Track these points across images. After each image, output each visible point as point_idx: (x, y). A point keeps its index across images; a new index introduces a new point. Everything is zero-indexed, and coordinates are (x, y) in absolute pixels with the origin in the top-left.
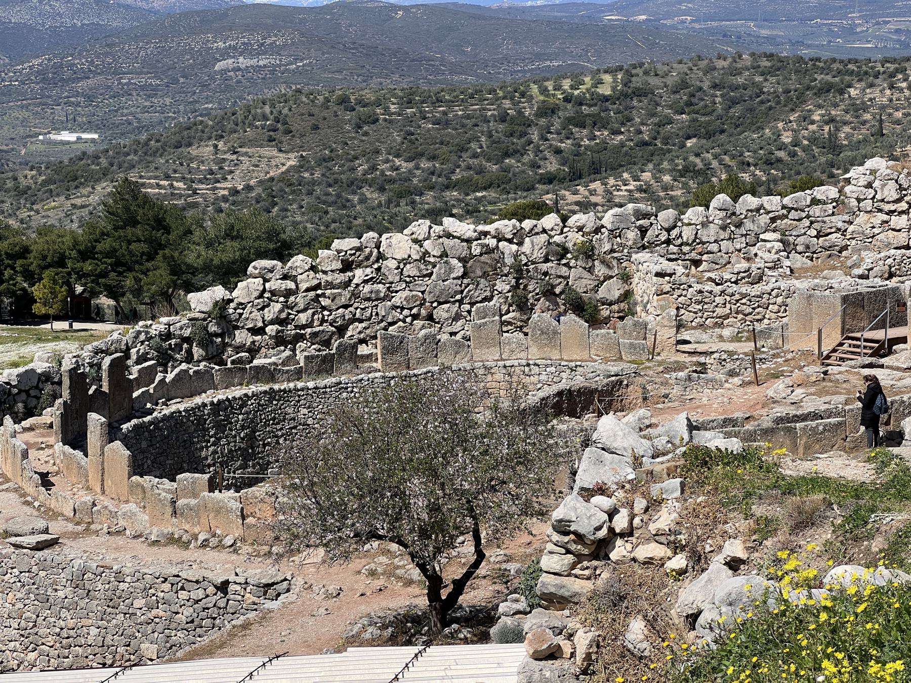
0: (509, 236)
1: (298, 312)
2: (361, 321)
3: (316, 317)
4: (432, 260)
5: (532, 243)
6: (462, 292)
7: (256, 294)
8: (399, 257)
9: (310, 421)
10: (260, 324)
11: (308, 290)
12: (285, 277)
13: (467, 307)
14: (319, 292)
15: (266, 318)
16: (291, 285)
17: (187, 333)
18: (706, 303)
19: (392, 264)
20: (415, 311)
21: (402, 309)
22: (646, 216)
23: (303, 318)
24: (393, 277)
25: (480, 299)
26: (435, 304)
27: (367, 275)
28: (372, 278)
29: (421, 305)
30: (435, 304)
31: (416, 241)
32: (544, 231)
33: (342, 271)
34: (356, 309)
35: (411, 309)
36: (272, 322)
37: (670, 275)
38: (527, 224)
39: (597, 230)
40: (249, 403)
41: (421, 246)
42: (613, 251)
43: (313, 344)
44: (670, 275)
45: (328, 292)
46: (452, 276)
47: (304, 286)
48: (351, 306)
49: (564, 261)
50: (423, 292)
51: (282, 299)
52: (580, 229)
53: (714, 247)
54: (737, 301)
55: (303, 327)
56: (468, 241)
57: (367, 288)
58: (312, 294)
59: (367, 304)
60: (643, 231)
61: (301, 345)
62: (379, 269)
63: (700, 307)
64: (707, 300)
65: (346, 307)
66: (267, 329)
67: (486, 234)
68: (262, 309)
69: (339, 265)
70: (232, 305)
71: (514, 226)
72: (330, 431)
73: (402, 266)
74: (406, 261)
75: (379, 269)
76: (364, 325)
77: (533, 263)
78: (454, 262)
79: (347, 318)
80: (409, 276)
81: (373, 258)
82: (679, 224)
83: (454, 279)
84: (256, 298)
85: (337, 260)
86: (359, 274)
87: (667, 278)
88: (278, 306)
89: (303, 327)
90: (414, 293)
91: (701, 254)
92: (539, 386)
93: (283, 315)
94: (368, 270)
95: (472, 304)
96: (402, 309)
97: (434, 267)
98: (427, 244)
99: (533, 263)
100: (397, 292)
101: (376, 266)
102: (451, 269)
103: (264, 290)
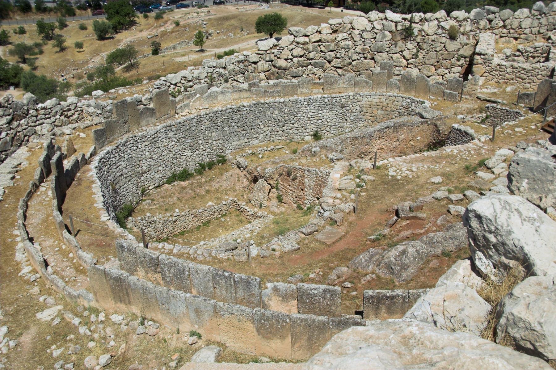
0: (417, 21)
1: (309, 52)
2: (339, 58)
3: (317, 55)
4: (376, 31)
6: (389, 47)
9: (279, 118)
10: (290, 57)
11: (315, 42)
13: (391, 55)
14: (320, 43)
15: (294, 55)
18: (501, 71)
19: (357, 32)
20: (365, 55)
21: (360, 53)
22: (494, 13)
23: (312, 55)
24: (357, 38)
25: (398, 51)
26: (376, 53)
31: (370, 21)
35: (363, 54)
36: (296, 57)
37: (484, 55)
38: (428, 15)
39: (465, 20)
40: (245, 109)
41: (372, 24)
42: (471, 31)
43: (315, 67)
44: (484, 55)
45: (324, 44)
49: (444, 35)
51: (302, 46)
52: (455, 19)
53: (528, 31)
54: (519, 72)
55: (312, 59)
56: (396, 22)
58: (317, 44)
59: (343, 50)
60: (490, 21)
61: (310, 67)
63: (497, 73)
64: (501, 70)
65: (332, 51)
66: (294, 59)
67: (405, 19)
69: (331, 31)
70: (278, 48)
71: (420, 16)
73: (361, 33)
74: (363, 31)
76: (340, 60)
77: (427, 35)
78: (387, 33)
81: (347, 29)
82: (511, 18)
84: (290, 45)
86: (340, 36)
87: (482, 56)
89: (312, 59)
91: (520, 35)
92: (401, 108)
93: (302, 53)
96: (360, 53)
97: (376, 34)
98: (375, 23)
99: (427, 35)
101: (348, 33)
102: (385, 36)
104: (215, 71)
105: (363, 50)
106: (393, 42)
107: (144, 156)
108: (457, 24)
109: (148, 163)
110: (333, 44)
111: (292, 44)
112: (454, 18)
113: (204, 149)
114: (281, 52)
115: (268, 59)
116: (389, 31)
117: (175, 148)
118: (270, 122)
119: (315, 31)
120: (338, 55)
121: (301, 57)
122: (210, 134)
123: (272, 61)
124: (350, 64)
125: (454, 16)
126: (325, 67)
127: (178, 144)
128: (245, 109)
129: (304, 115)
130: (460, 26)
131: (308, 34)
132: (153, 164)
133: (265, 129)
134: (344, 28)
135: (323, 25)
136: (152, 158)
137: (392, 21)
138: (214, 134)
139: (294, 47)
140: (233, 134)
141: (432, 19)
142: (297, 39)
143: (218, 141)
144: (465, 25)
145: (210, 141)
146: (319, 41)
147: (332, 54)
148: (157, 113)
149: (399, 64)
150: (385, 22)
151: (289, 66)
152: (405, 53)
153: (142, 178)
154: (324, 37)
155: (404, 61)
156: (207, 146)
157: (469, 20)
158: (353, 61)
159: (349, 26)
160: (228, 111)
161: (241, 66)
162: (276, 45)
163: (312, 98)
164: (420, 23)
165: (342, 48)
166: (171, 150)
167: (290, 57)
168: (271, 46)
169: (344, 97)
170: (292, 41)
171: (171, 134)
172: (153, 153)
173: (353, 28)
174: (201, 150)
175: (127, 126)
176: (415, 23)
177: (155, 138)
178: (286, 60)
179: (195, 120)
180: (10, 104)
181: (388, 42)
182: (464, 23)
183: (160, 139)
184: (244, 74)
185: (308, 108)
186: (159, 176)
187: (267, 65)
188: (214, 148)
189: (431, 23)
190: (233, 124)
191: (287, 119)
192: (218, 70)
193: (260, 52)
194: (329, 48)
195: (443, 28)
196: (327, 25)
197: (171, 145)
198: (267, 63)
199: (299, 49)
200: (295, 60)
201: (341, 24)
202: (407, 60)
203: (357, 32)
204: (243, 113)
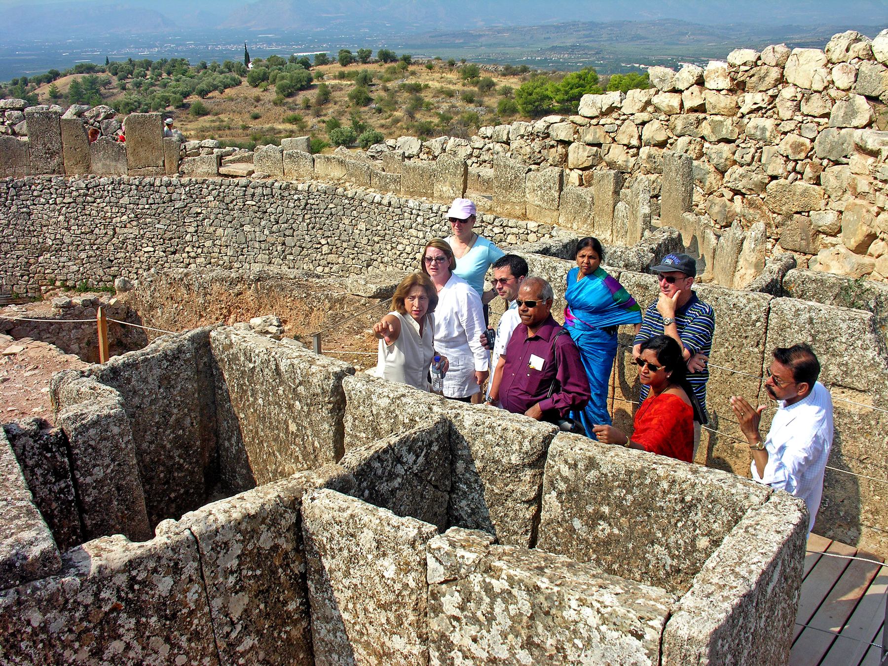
3: (692, 146)
7: (641, 104)
10: (635, 142)
11: (693, 110)
14: (701, 116)
17: (563, 136)
27: (755, 104)
28: (760, 108)
30: (825, 162)
33: (731, 91)
34: (738, 146)
46: (855, 123)
47: (687, 105)
48: (734, 141)
50: (813, 140)
51: (663, 117)
57: (754, 122)
58: (693, 116)
62: (774, 97)
65: (728, 141)
68: (643, 123)
69: (725, 84)
70: (615, 115)
72: (379, 260)
76: (741, 170)
78: (861, 101)
79: (725, 156)
80: (803, 114)
83: (857, 128)
85: (725, 77)
86: (750, 100)
90: (802, 140)
93: (661, 137)
100: (785, 133)
101: (770, 92)
102: (852, 113)
103: (648, 103)
104: (486, 147)
105: (797, 147)
107: (54, 220)
109: (58, 236)
110: (729, 121)
111: (643, 109)
113: (192, 254)
114: (619, 126)
115: (589, 138)
116: (869, 98)
117: (126, 230)
118: (345, 245)
119: (693, 80)
120: (737, 157)
121: (662, 145)
122: (212, 229)
123: (599, 145)
124: (763, 187)
126: (707, 184)
127: (135, 223)
128: (296, 197)
129: (408, 249)
131: (681, 87)
132: (70, 241)
133: (332, 258)
134: (762, 79)
135: (714, 65)
136: (68, 229)
138: (220, 231)
139: (645, 116)
140: (257, 245)
143: (224, 249)
145: (208, 243)
146: (701, 108)
147: (725, 148)
148: (131, 158)
151: (631, 165)
153: (41, 259)
154: (711, 98)
156: (200, 250)
158: (774, 178)
159: (774, 73)
160: (259, 191)
161: (537, 144)
162: (616, 107)
163: (435, 208)
165: (752, 137)
166: (117, 229)
167: (635, 142)
168: (604, 110)
169: (515, 230)
170: (645, 99)
171: (125, 200)
172: (73, 221)
173: (782, 80)
174: (185, 255)
175: (57, 160)
177: (86, 195)
178: (629, 147)
179: (187, 189)
180: (99, 122)
183: (98, 201)
184: (538, 164)
185: (421, 235)
186: (75, 268)
187: (586, 154)
188: (213, 260)
190: (263, 223)
191: (377, 247)
192: (491, 145)
193: (577, 119)
194: (720, 131)
196: (726, 65)
197: (118, 219)
198: (588, 148)
199: (656, 124)
201: (756, 65)
203: (787, 92)
204: (291, 205)
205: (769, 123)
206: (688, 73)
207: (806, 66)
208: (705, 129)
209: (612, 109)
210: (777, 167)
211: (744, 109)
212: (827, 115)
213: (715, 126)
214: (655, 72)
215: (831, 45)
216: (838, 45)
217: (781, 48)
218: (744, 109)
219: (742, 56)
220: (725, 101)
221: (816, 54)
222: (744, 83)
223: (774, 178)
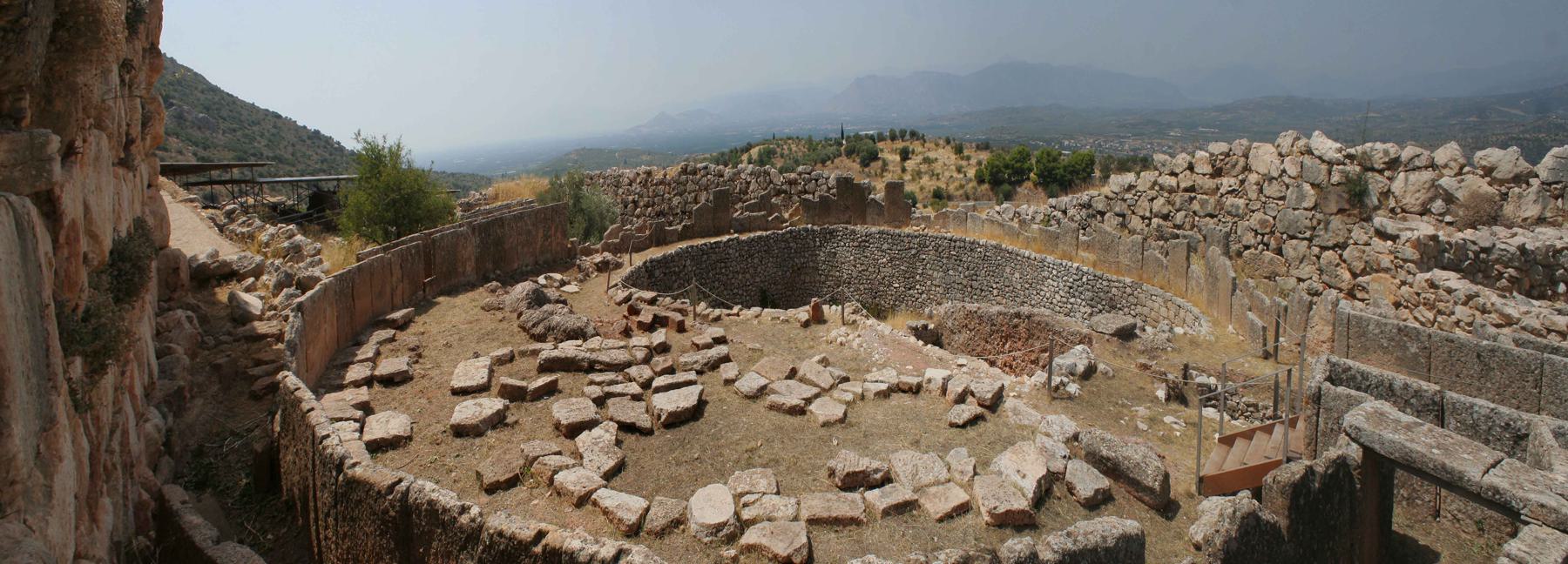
1: (1178, 211)
5: (1407, 179)
6: (1314, 229)
8: (1263, 170)
11: (1186, 190)
12: (1173, 174)
16: (1172, 181)
19: (1253, 178)
25: (1330, 244)
29: (1272, 233)
32: (1432, 166)
33: (1212, 176)
39: (1520, 179)
46: (1305, 205)
47: (1183, 185)
49: (1448, 218)
52: (1488, 171)
56: (1330, 163)
57: (1230, 201)
58: (1187, 195)
59: (1229, 218)
65: (1212, 216)
68: (1152, 200)
69: (1208, 169)
71: (1386, 152)
75: (1242, 182)
77: (1403, 211)
78: (1307, 187)
86: (1227, 182)
88: (1161, 201)
93: (1165, 211)
94: (1232, 181)
95: (1324, 248)
99: (1403, 211)
102: (1302, 197)
103: (1155, 183)
105: (1263, 223)
106: (1319, 216)
108: (1491, 190)
110: (1212, 200)
112: (1484, 168)
115: (1117, 209)
116: (1313, 185)
121: (1166, 217)
123: (1123, 216)
125: (1484, 163)
130: (1504, 197)
134: (1234, 166)
135: (1200, 154)
137: (1320, 158)
141: (1417, 163)
142: (1160, 180)
144: (1520, 196)
146: (1191, 189)
149: (1333, 281)
150: (1307, 160)
152: (1346, 254)
154: (1200, 181)
155: (1347, 275)
157: (1532, 181)
158: (1247, 248)
159: (1242, 162)
164: (1387, 173)
165: (1229, 213)
173: (1247, 168)
176: (1373, 169)
178: (1143, 218)
181: (1310, 214)
182: (1517, 190)
189: (1413, 177)
195: (1449, 199)
199: (1161, 201)
200: (1155, 221)
202: (1355, 276)
203: (1253, 178)
205: (1241, 202)
206: (1182, 159)
207: (1265, 157)
208: (1196, 206)
209: (1131, 187)
210: (1249, 239)
211: (1222, 190)
212: (1283, 198)
213: (1203, 203)
214: (1159, 157)
215: (1279, 140)
216: (1285, 140)
217: (1245, 142)
218: (1222, 190)
219: (1219, 147)
220: (1210, 183)
221: (1269, 148)
222: (1221, 169)
223: (1247, 248)
